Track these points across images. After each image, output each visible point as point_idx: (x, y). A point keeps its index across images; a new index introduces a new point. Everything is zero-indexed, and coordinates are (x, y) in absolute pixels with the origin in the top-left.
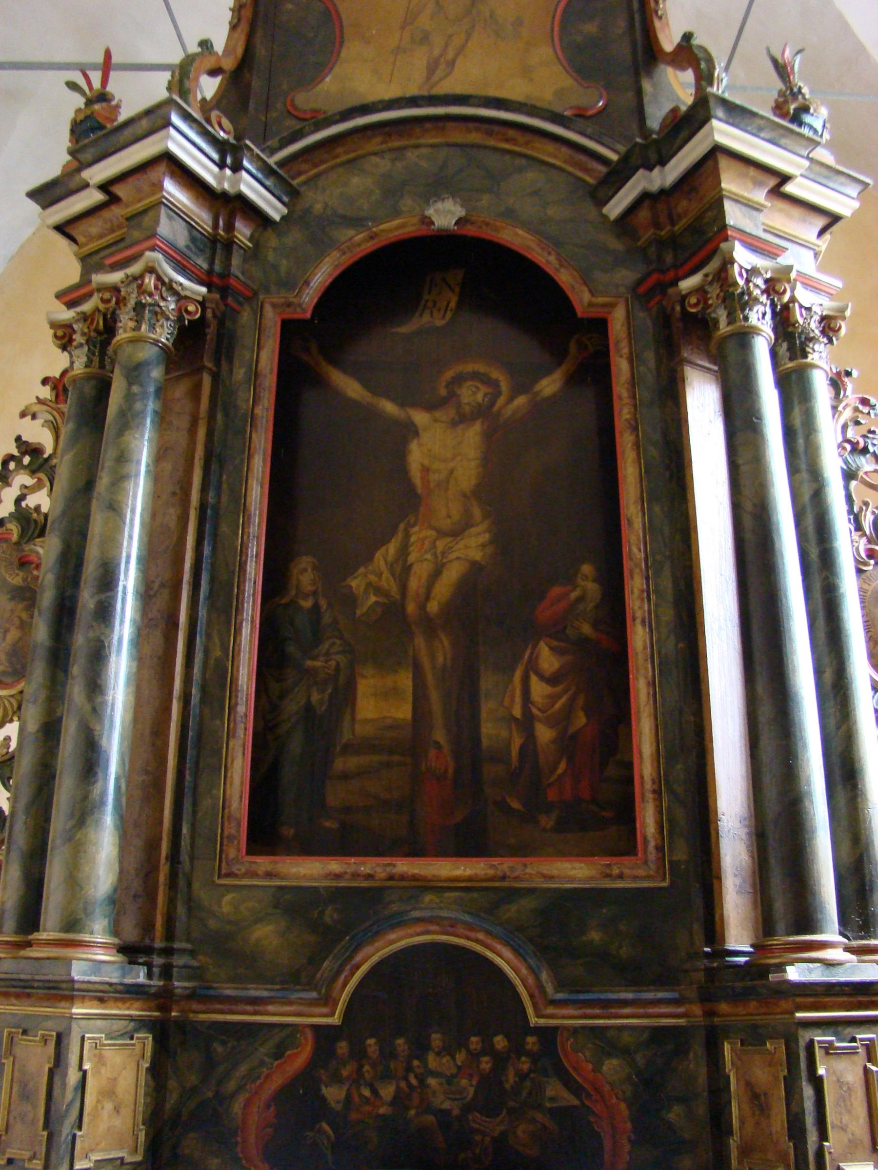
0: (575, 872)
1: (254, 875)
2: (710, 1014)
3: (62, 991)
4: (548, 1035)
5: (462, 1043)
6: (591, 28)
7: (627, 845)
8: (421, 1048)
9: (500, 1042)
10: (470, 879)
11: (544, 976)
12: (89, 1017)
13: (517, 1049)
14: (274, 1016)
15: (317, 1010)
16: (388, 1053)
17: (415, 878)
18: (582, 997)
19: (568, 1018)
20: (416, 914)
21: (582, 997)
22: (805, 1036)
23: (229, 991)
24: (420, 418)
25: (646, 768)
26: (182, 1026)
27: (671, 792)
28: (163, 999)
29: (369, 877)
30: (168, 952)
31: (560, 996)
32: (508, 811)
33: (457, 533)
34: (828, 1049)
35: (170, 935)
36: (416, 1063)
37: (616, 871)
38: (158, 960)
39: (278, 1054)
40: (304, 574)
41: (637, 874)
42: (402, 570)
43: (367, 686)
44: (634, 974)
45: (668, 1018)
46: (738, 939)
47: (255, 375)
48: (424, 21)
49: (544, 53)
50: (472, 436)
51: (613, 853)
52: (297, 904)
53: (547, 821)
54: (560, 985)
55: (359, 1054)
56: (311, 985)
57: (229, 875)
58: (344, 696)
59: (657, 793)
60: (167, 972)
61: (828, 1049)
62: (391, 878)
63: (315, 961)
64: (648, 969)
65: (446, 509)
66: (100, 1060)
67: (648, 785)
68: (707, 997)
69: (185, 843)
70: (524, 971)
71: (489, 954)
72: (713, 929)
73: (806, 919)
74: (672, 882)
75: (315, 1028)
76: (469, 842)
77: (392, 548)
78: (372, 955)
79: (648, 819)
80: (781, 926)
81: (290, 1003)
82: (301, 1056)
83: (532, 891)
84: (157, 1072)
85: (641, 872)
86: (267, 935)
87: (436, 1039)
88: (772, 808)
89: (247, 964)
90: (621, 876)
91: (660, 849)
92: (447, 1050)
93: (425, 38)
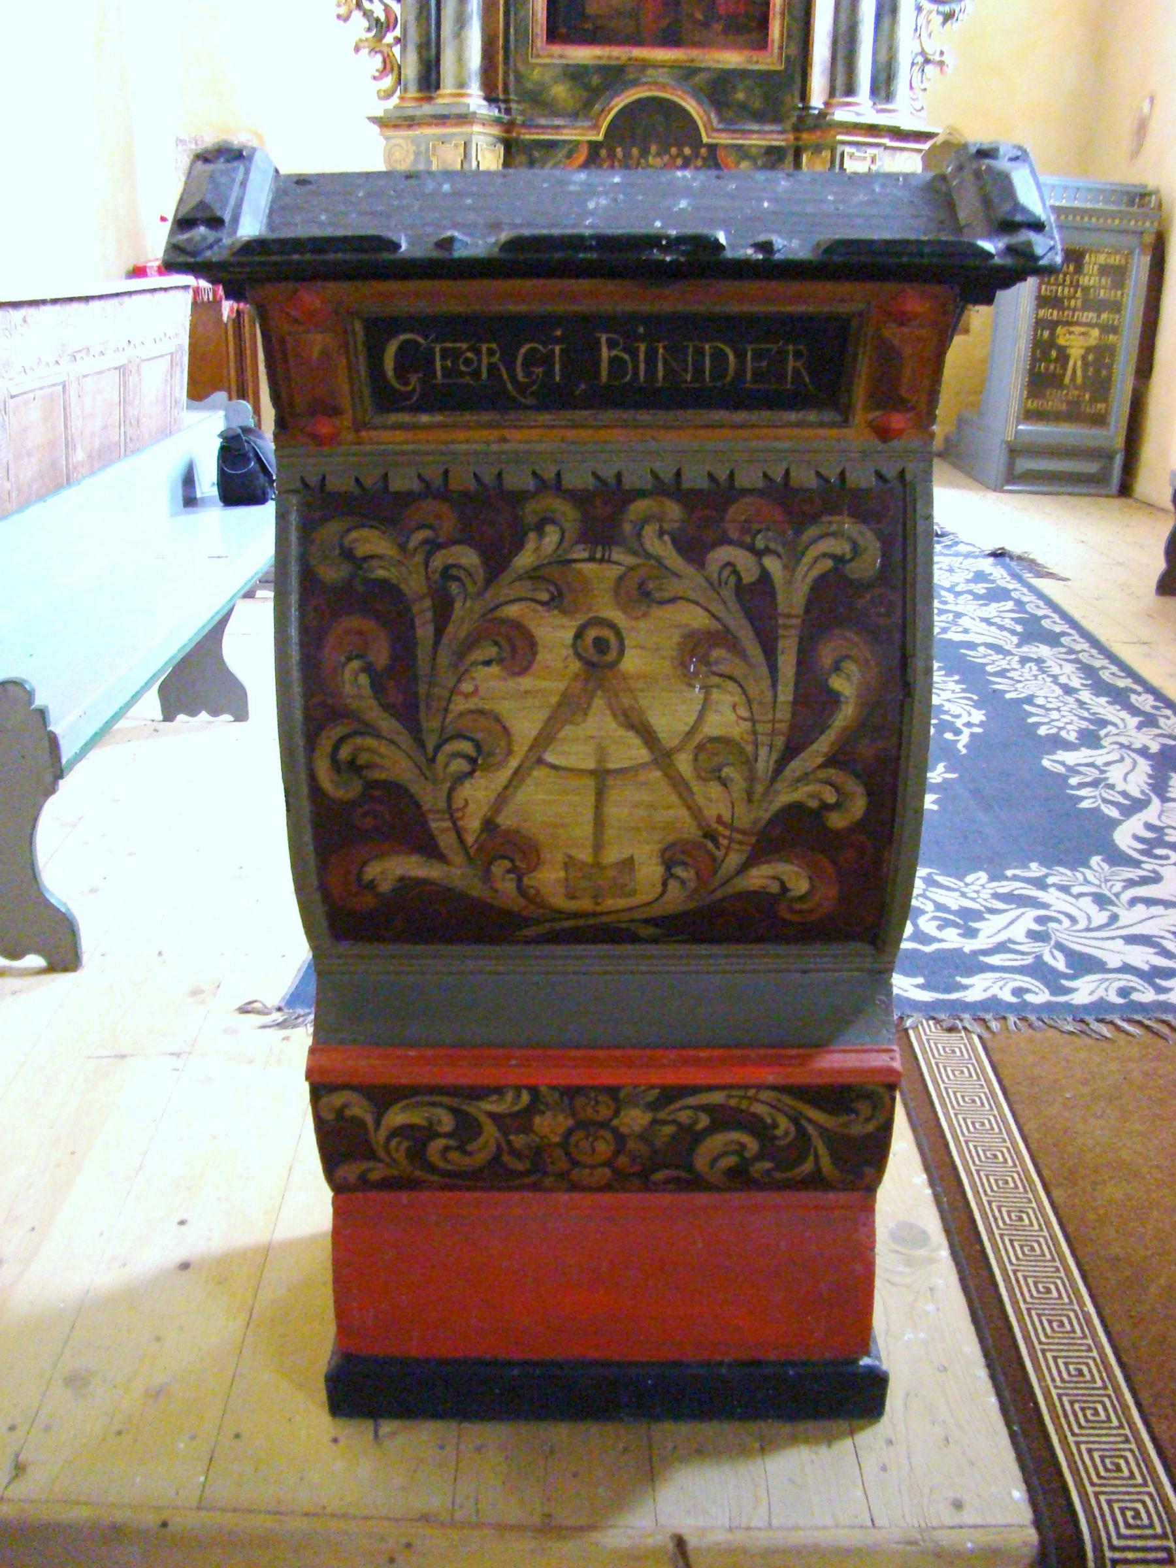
0: (731, 59)
1: (552, 56)
2: (797, 139)
3: (465, 118)
4: (713, 148)
5: (667, 152)
7: (762, 44)
8: (645, 152)
9: (687, 151)
10: (675, 61)
11: (713, 116)
12: (479, 133)
13: (696, 154)
14: (567, 135)
15: (590, 132)
16: (627, 155)
17: (644, 60)
18: (732, 127)
19: (724, 139)
20: (644, 80)
21: (732, 127)
22: (840, 149)
23: (543, 122)
26: (516, 140)
27: (790, 14)
28: (509, 126)
29: (618, 58)
30: (506, 101)
31: (721, 126)
32: (696, 22)
34: (851, 156)
35: (506, 90)
36: (643, 161)
37: (755, 59)
38: (503, 106)
39: (569, 156)
41: (768, 61)
44: (759, 117)
45: (778, 141)
46: (817, 100)
51: (754, 49)
52: (576, 74)
53: (718, 27)
54: (721, 120)
55: (612, 156)
56: (587, 117)
57: (538, 56)
59: (783, 14)
60: (508, 111)
61: (851, 156)
62: (630, 59)
63: (588, 105)
64: (770, 113)
66: (483, 155)
67: (778, 9)
68: (797, 129)
69: (512, 38)
70: (702, 113)
71: (683, 104)
72: (804, 95)
73: (850, 90)
74: (786, 68)
75: (590, 143)
76: (671, 39)
78: (620, 103)
79: (775, 29)
80: (838, 93)
81: (576, 128)
83: (708, 69)
85: (769, 60)
86: (560, 91)
87: (653, 149)
88: (843, 27)
89: (549, 107)
90: (757, 62)
91: (781, 48)
92: (658, 154)
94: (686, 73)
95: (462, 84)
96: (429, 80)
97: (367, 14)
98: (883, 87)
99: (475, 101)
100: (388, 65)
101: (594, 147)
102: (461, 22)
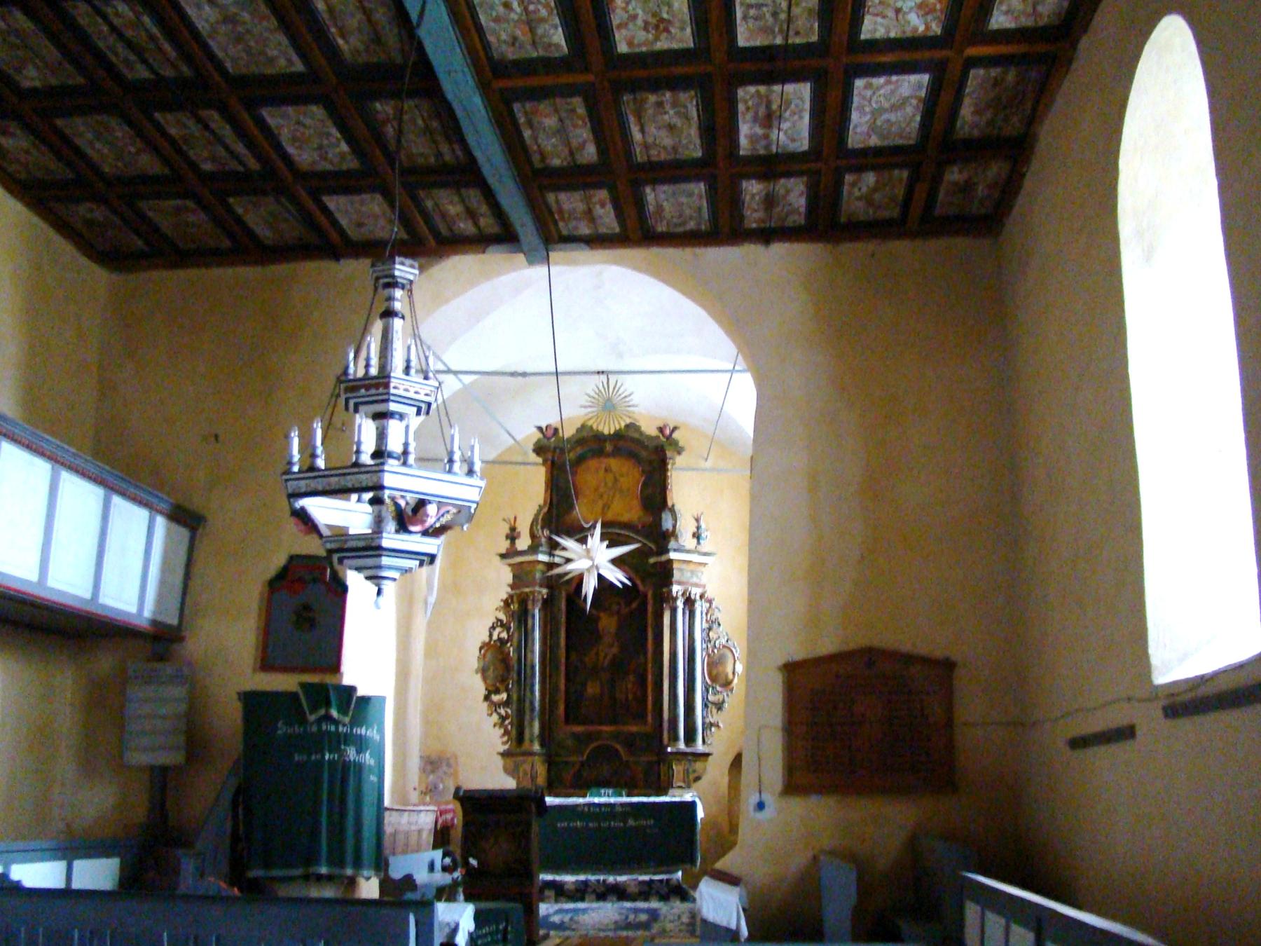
0: (634, 729)
3: (531, 754)
6: (650, 491)
24: (602, 614)
25: (650, 707)
33: (611, 646)
40: (573, 656)
41: (647, 729)
42: (597, 654)
43: (589, 684)
47: (560, 610)
48: (602, 490)
49: (636, 503)
50: (615, 618)
52: (576, 736)
58: (584, 685)
65: (607, 640)
73: (676, 739)
76: (614, 722)
77: (595, 651)
78: (592, 746)
79: (650, 718)
82: (577, 767)
84: (549, 771)
86: (570, 742)
93: (602, 496)
94: (616, 736)
95: (532, 741)
96: (520, 739)
97: (499, 714)
98: (690, 738)
99: (536, 747)
100: (506, 733)
101: (582, 764)
102: (532, 719)
